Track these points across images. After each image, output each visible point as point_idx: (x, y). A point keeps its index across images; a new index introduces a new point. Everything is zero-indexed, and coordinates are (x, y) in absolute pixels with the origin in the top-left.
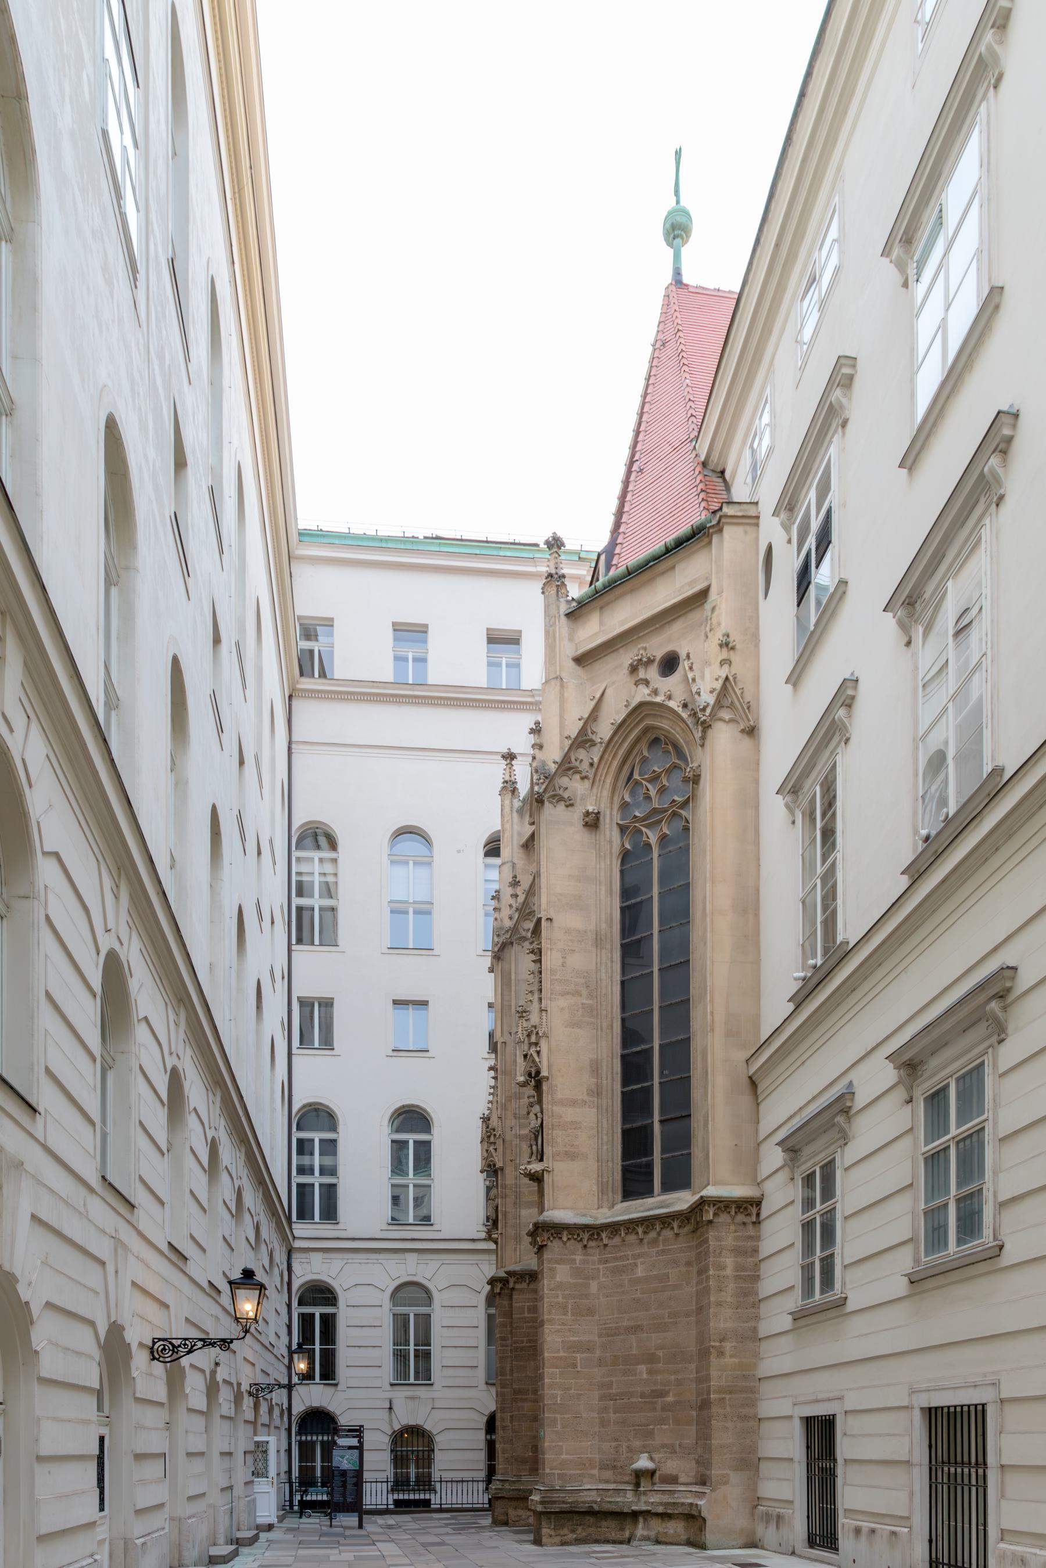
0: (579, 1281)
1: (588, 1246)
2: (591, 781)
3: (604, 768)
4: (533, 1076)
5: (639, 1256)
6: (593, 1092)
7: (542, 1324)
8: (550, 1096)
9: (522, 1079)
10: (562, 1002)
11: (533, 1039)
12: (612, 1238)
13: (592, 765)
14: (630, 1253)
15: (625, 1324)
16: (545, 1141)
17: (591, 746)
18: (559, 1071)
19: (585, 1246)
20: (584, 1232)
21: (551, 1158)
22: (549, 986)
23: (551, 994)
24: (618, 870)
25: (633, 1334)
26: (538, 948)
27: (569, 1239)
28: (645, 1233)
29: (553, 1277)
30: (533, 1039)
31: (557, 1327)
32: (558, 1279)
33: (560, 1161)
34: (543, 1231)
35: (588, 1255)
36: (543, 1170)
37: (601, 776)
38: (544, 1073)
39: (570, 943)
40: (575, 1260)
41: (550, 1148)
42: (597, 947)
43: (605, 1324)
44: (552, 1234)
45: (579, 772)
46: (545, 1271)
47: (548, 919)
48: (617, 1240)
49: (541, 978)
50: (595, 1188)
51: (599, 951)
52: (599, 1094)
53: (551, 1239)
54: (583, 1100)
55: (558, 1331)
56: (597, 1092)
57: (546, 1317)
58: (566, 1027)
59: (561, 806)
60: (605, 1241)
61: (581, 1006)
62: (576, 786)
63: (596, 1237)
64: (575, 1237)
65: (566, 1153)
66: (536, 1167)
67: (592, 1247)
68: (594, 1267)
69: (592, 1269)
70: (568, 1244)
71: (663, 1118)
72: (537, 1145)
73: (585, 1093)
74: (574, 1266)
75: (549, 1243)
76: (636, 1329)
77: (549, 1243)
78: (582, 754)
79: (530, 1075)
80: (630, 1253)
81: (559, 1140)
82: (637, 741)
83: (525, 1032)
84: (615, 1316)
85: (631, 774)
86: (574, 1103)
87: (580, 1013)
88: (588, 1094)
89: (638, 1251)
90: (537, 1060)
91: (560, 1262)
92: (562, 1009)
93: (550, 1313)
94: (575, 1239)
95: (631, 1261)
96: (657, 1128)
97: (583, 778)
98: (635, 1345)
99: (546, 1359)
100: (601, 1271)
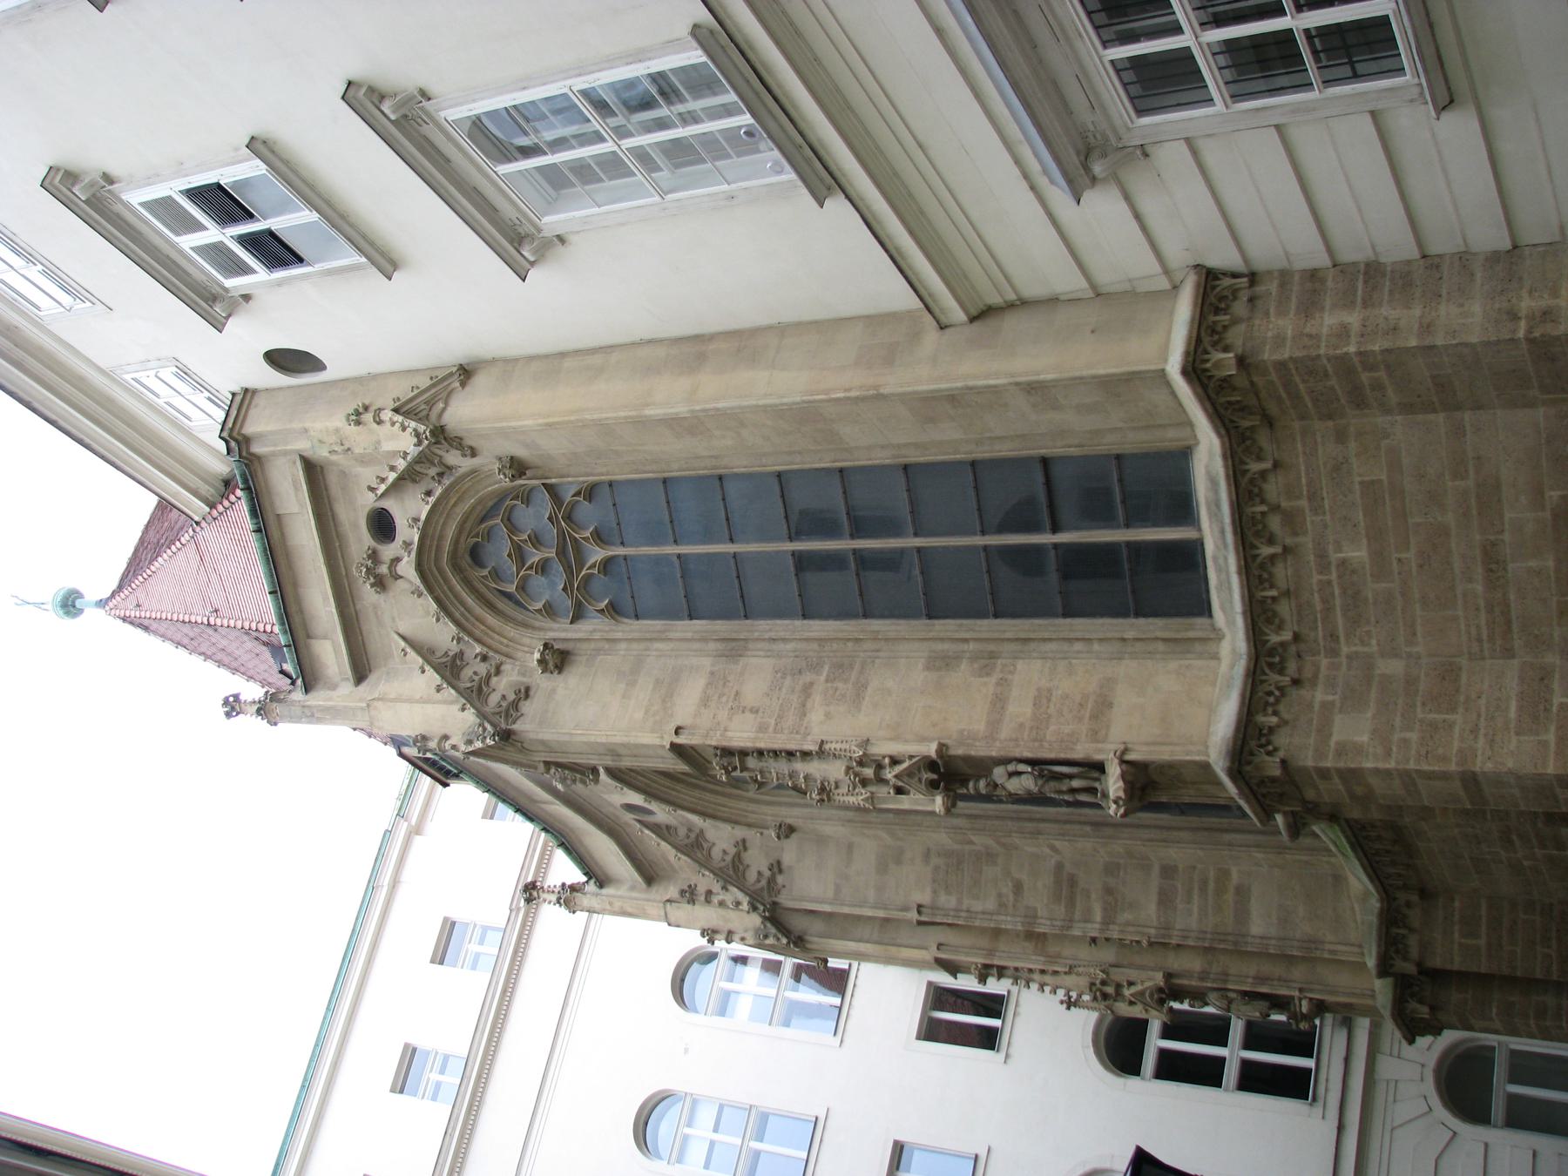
0: (1374, 694)
1: (1296, 676)
2: (504, 659)
3: (492, 639)
4: (935, 776)
5: (1322, 556)
6: (986, 666)
7: (1471, 781)
8: (977, 744)
9: (939, 800)
10: (816, 716)
11: (869, 772)
12: (1282, 622)
13: (484, 658)
14: (1316, 578)
15: (1479, 588)
16: (1062, 756)
17: (462, 659)
18: (934, 725)
19: (1296, 682)
20: (1262, 682)
21: (1100, 745)
22: (784, 737)
23: (797, 733)
24: (636, 622)
25: (1505, 569)
26: (721, 756)
27: (1275, 713)
28: (1271, 541)
29: (1359, 750)
30: (869, 772)
31: (1481, 742)
32: (1365, 738)
33: (1108, 727)
34: (1249, 763)
35: (1316, 676)
36: (1123, 762)
37: (502, 643)
38: (931, 750)
39: (724, 699)
40: (1324, 705)
41: (1079, 747)
42: (740, 656)
43: (1480, 640)
44: (1261, 746)
45: (489, 677)
46: (1341, 765)
47: (677, 733)
48: (1284, 609)
49: (769, 751)
50: (1173, 665)
51: (749, 653)
52: (993, 656)
53: (1270, 748)
54: (998, 684)
55: (1492, 742)
56: (986, 661)
57: (1453, 767)
58: (860, 711)
59: (526, 707)
60: (1286, 636)
61: (829, 685)
62: (503, 685)
63: (1277, 659)
64: (1271, 699)
65: (1095, 717)
66: (1114, 784)
67: (1300, 670)
68: (1344, 668)
69: (1349, 668)
70: (1286, 716)
71: (1047, 523)
72: (1071, 777)
73: (985, 679)
74: (1338, 704)
75: (1281, 754)
76: (1492, 559)
77: (1281, 754)
78: (467, 673)
79: (934, 785)
80: (1316, 578)
81: (1067, 729)
82: (468, 583)
83: (857, 790)
84: (1460, 613)
85: (508, 596)
86: (999, 703)
87: (840, 685)
88: (988, 674)
89: (1312, 558)
90: (905, 765)
91: (1324, 731)
92: (828, 715)
93: (1444, 759)
94: (1278, 701)
95: (1334, 576)
96: (1063, 537)
97: (498, 672)
98: (1532, 563)
99: (1559, 772)
100: (1354, 649)
